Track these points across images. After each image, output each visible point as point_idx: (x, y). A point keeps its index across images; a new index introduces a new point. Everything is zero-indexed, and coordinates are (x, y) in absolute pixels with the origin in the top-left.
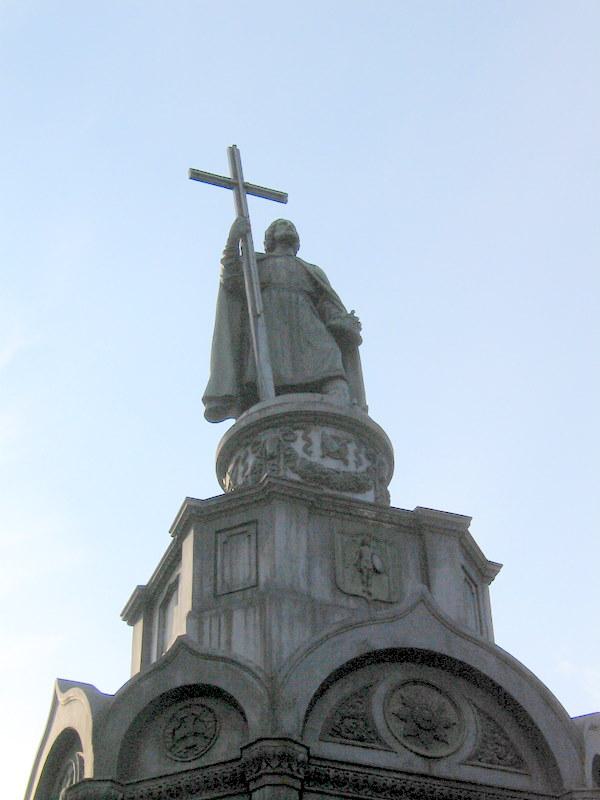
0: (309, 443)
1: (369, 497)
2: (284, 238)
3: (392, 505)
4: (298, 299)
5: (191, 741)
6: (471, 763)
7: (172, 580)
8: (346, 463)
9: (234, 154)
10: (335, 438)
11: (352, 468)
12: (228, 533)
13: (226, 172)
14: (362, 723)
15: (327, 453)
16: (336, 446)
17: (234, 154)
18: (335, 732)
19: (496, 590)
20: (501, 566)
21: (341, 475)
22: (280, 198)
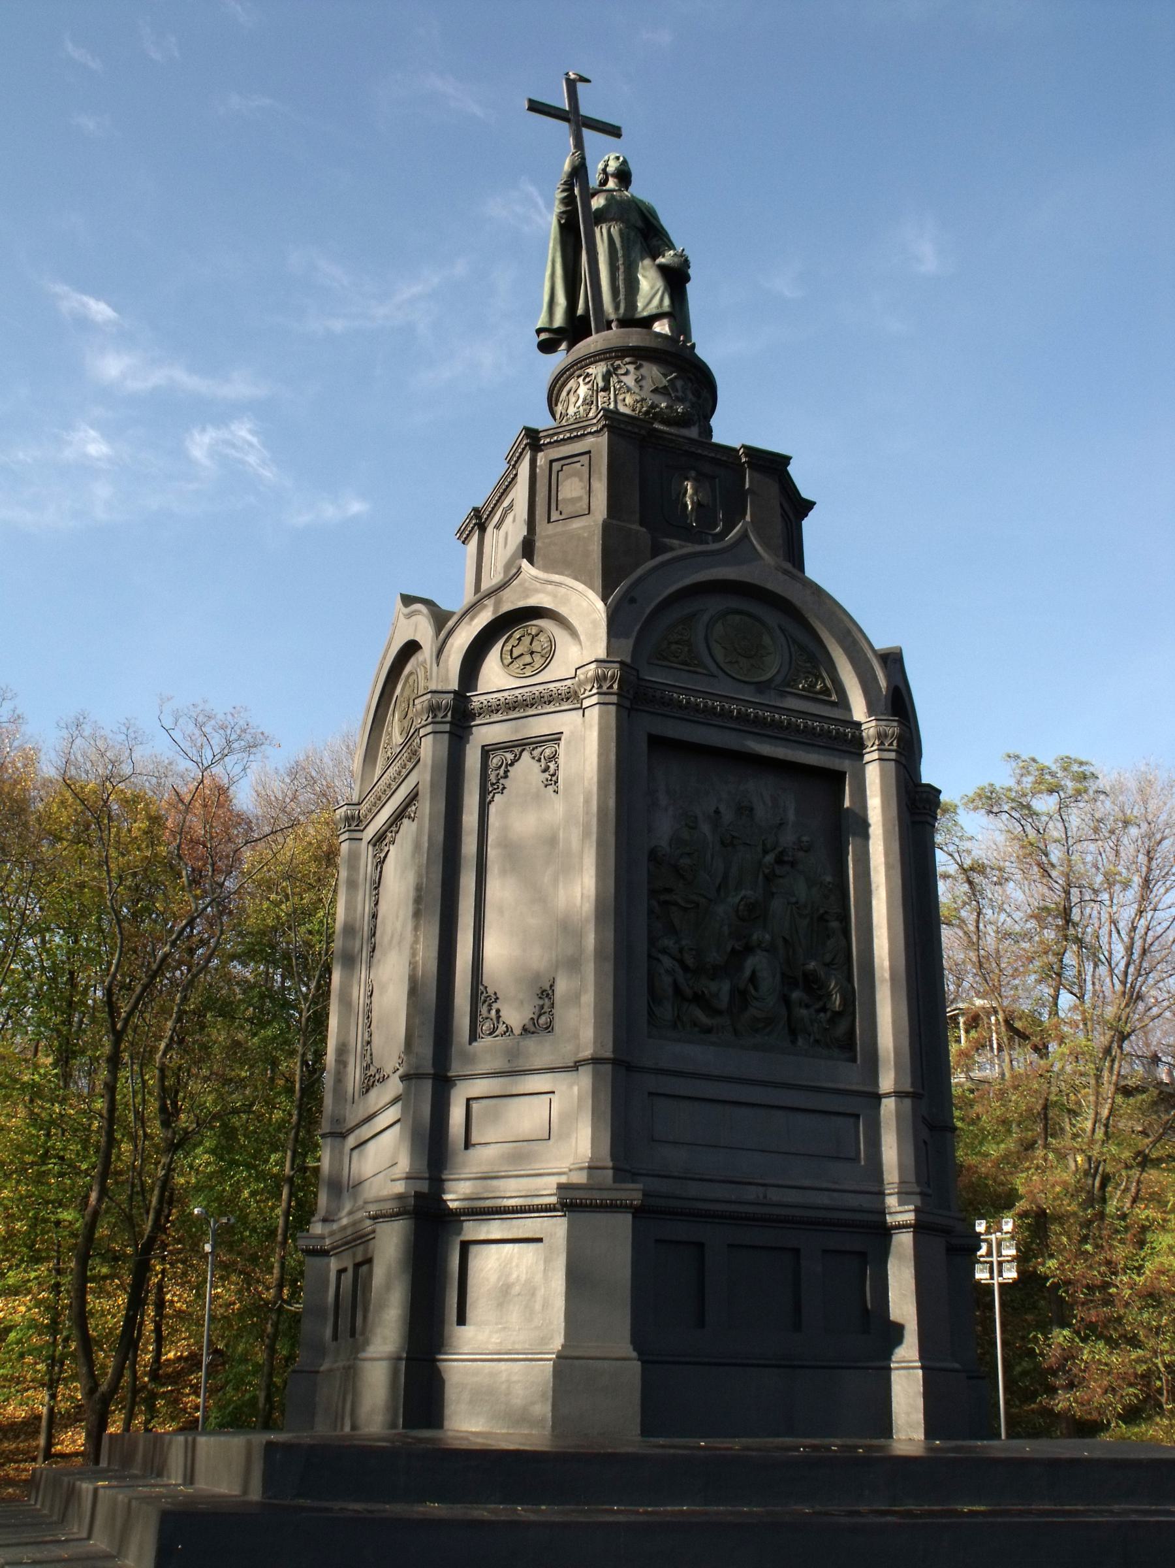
1: (693, 432)
3: (714, 440)
5: (528, 659)
7: (506, 504)
12: (563, 462)
19: (810, 526)
20: (814, 503)
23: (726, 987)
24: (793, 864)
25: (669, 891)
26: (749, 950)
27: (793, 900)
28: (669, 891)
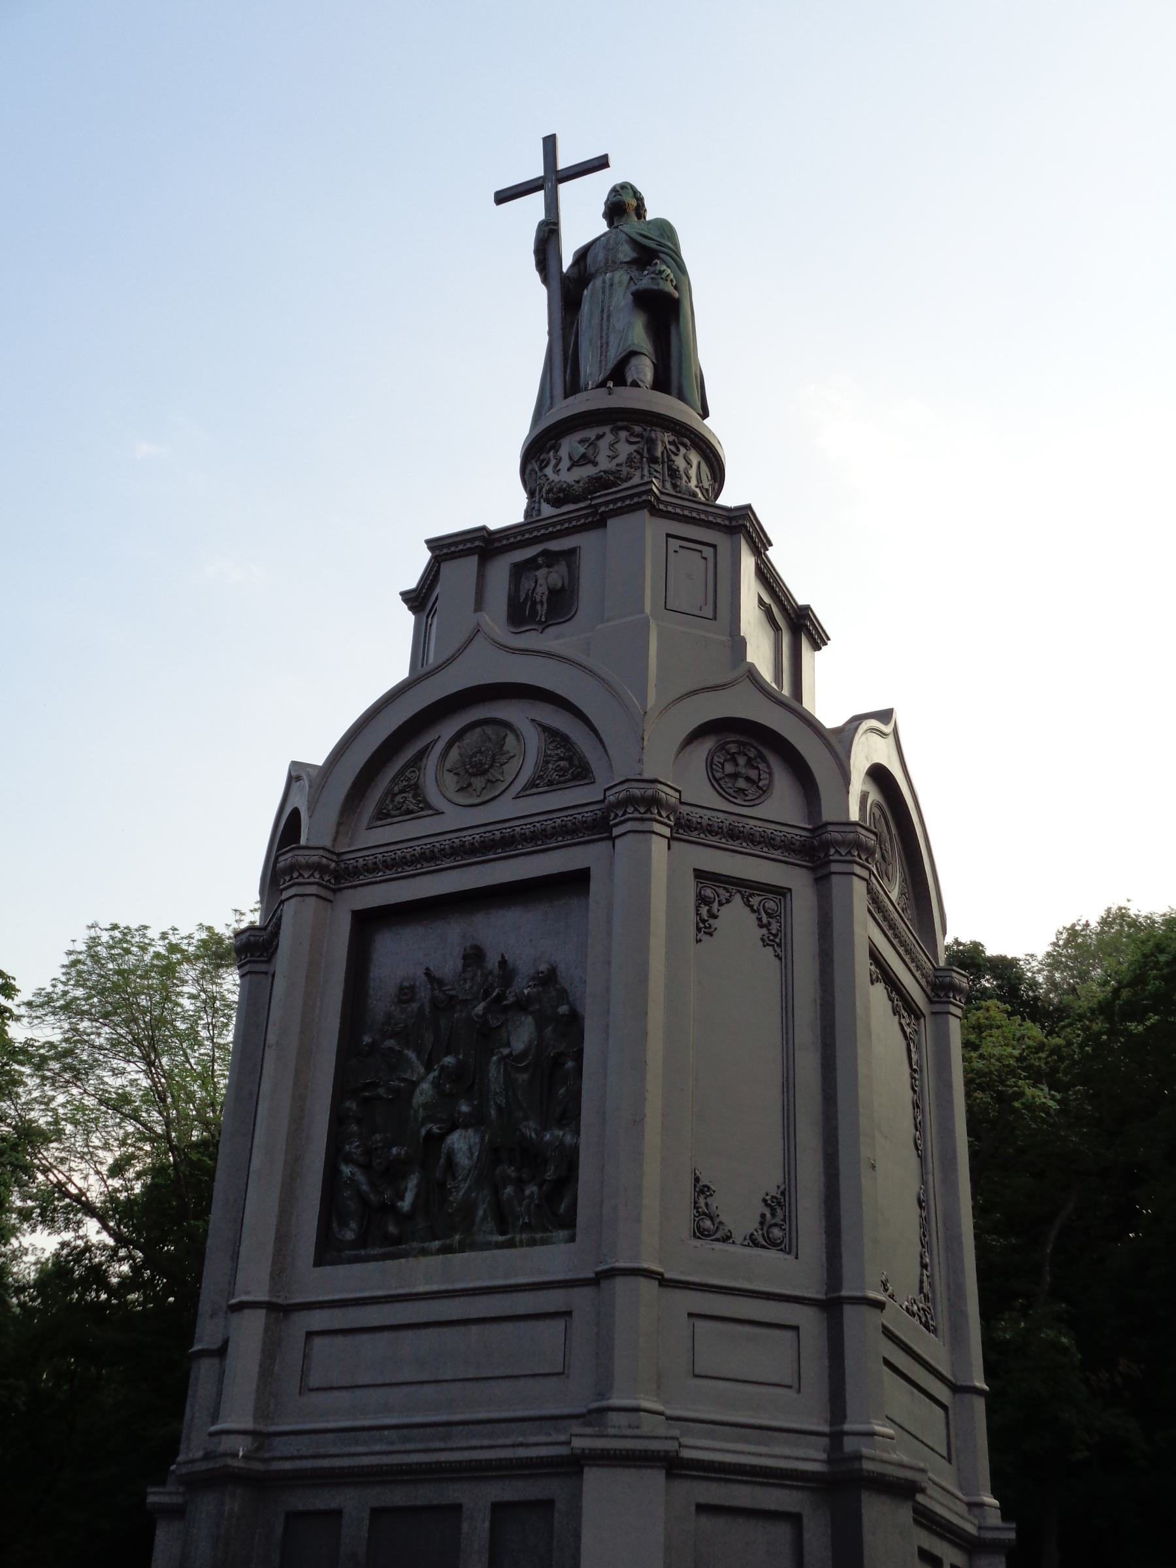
0: (559, 460)
2: (623, 206)
4: (612, 279)
6: (528, 792)
8: (595, 464)
9: (550, 143)
10: (582, 441)
11: (604, 464)
13: (536, 170)
14: (409, 796)
15: (574, 464)
16: (582, 450)
17: (550, 143)
18: (382, 815)
21: (581, 484)
22: (601, 163)
23: (412, 1182)
24: (522, 1005)
25: (374, 1085)
26: (453, 1128)
27: (506, 1051)
28: (374, 1085)
